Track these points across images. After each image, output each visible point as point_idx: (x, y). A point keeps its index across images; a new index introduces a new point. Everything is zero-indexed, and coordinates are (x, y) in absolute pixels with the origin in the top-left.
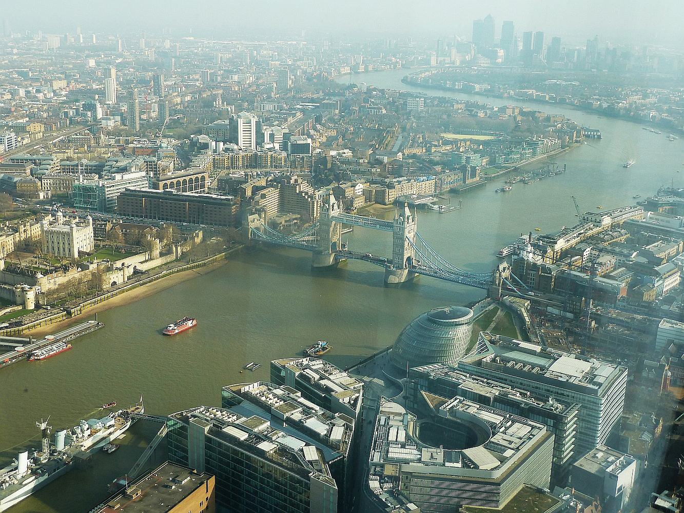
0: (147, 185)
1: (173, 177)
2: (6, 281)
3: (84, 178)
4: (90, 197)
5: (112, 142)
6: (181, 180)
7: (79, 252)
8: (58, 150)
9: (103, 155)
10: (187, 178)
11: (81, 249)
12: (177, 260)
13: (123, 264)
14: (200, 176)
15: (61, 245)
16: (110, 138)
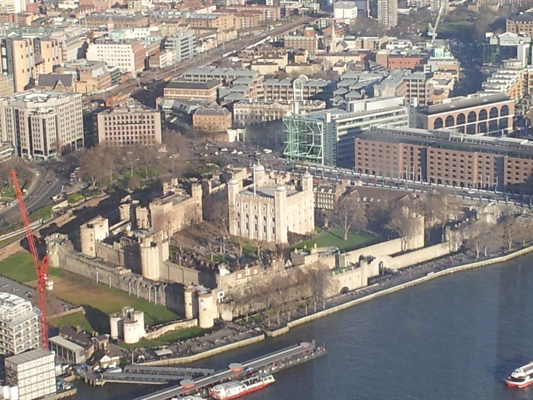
0: (408, 121)
1: (452, 106)
2: (171, 278)
3: (302, 107)
4: (310, 139)
5: (352, 45)
6: (466, 111)
7: (289, 234)
8: (262, 60)
9: (335, 69)
10: (477, 109)
11: (292, 230)
12: (452, 253)
13: (361, 258)
14: (499, 105)
15: (261, 219)
16: (348, 40)
